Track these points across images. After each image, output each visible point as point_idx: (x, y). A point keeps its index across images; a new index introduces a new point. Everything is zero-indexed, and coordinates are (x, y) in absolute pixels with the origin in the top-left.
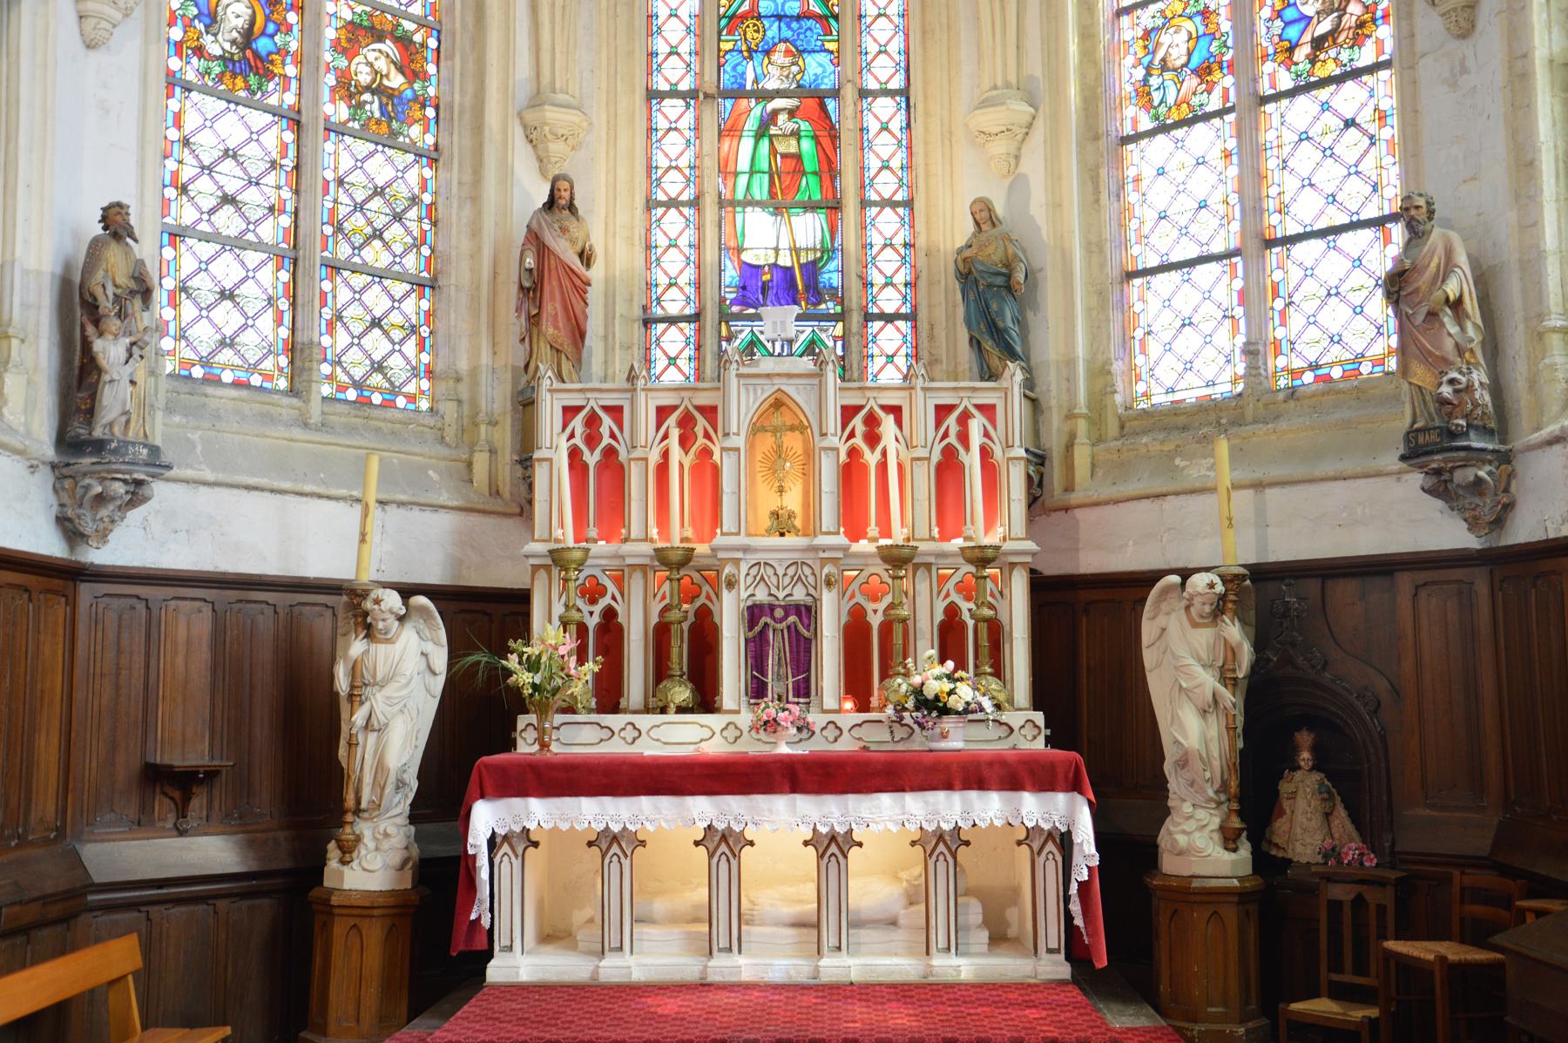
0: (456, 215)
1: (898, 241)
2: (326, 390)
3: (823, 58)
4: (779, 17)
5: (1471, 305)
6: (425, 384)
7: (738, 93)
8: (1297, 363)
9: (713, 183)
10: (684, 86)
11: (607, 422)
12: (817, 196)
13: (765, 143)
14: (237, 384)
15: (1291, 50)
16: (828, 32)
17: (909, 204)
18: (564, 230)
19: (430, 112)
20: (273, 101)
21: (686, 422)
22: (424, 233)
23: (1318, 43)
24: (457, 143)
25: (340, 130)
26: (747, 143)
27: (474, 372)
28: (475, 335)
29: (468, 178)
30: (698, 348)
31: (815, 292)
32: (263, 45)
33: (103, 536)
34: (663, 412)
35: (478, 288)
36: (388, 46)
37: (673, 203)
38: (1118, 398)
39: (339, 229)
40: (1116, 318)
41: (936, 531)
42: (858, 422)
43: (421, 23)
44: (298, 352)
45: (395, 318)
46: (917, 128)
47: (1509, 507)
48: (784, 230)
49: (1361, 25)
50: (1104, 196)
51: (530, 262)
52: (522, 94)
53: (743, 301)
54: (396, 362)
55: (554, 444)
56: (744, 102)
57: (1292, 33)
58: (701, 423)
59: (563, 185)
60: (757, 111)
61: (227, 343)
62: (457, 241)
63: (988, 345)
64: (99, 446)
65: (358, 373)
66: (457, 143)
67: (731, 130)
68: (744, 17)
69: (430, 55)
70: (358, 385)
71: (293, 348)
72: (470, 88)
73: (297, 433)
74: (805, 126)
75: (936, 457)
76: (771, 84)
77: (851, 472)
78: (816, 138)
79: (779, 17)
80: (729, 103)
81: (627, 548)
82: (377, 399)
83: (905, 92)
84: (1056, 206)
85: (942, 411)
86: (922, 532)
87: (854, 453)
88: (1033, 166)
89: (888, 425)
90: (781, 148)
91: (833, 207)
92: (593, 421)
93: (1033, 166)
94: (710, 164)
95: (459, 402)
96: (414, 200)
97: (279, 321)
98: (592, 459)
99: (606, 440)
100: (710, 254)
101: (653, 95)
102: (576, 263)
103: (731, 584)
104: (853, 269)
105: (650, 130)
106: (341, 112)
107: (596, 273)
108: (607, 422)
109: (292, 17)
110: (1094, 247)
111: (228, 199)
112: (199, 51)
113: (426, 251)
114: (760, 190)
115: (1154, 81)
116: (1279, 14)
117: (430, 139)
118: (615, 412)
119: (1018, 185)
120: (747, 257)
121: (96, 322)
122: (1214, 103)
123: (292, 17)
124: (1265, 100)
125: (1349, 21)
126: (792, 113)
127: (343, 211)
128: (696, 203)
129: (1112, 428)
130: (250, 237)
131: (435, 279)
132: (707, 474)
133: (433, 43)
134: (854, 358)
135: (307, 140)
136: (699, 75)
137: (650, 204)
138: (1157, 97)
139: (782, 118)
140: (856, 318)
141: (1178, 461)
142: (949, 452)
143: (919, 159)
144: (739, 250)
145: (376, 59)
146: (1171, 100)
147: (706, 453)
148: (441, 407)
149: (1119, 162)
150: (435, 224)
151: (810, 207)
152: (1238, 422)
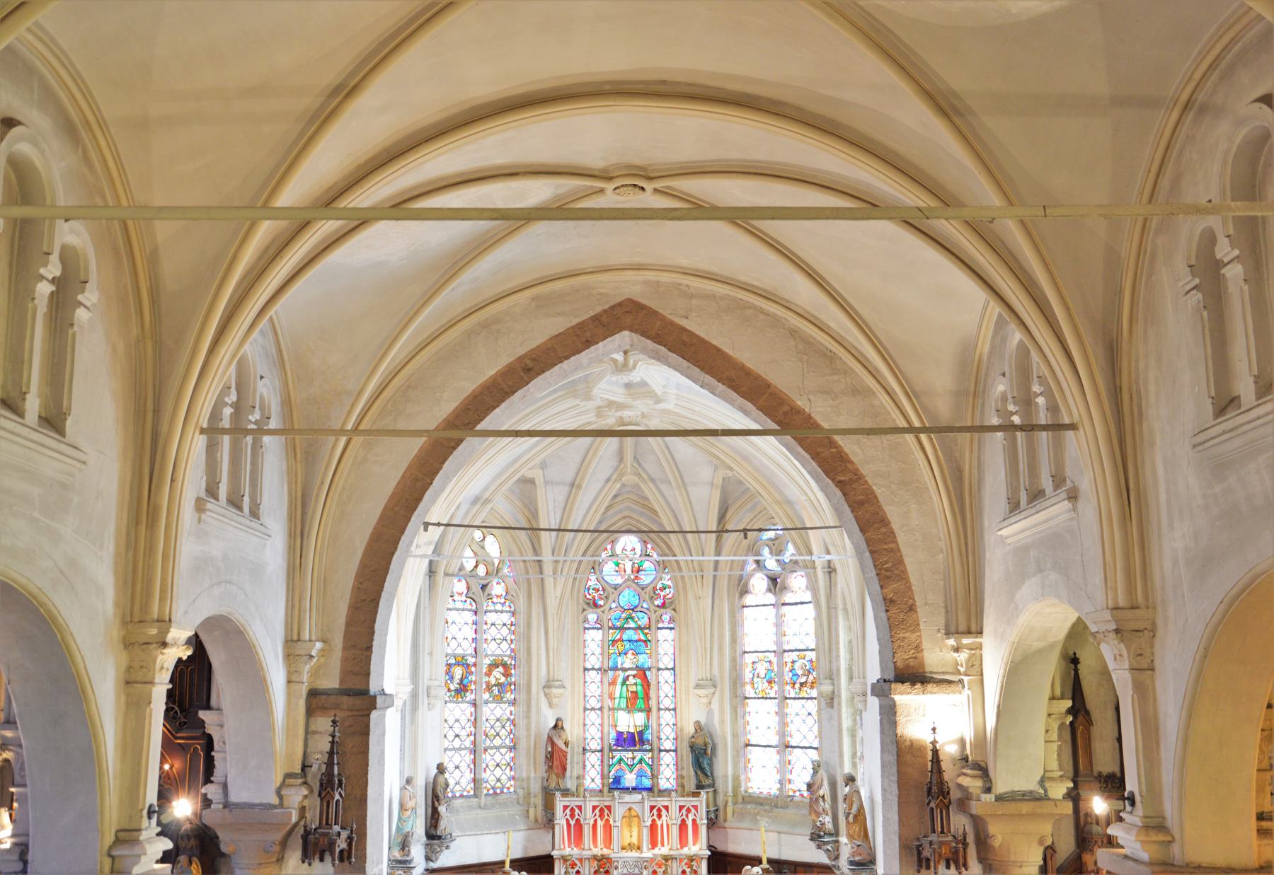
0: (521, 723)
1: (671, 723)
2: (485, 792)
3: (645, 656)
4: (630, 641)
5: (828, 798)
6: (512, 782)
7: (615, 669)
8: (795, 789)
9: (608, 703)
10: (596, 667)
11: (577, 811)
12: (643, 707)
13: (625, 687)
14: (461, 796)
15: (794, 684)
16: (647, 646)
17: (675, 709)
18: (560, 736)
19: (513, 687)
20: (468, 699)
21: (602, 810)
22: (511, 730)
23: (802, 684)
24: (522, 698)
25: (486, 702)
26: (618, 687)
27: (528, 778)
28: (528, 765)
29: (525, 709)
30: (602, 762)
31: (642, 742)
32: (465, 681)
33: (437, 859)
34: (594, 808)
35: (529, 749)
36: (501, 669)
37: (593, 709)
38: (742, 789)
39: (487, 736)
40: (742, 760)
41: (679, 847)
42: (655, 811)
43: (510, 657)
44: (476, 781)
45: (504, 762)
46: (677, 682)
47: (839, 855)
48: (632, 719)
49: (813, 683)
50: (739, 718)
51: (550, 749)
52: (543, 683)
53: (617, 745)
54: (504, 778)
55: (560, 820)
56: (617, 672)
57: (795, 678)
58: (606, 811)
59: (560, 722)
60: (621, 675)
61: (457, 783)
62: (522, 733)
63: (699, 772)
64: (439, 838)
65: (493, 784)
66: (522, 698)
67: (613, 683)
68: (617, 641)
69: (513, 667)
70: (493, 788)
71: (474, 780)
72: (526, 678)
73: (479, 811)
74: (639, 681)
75: (679, 822)
76: (627, 665)
77: (653, 827)
78: (642, 685)
79: (630, 641)
80: (612, 672)
81: (584, 853)
82: (498, 791)
83: (673, 669)
84: (722, 722)
85: (681, 808)
86: (674, 847)
87: (654, 821)
88: (715, 706)
89: (664, 811)
90: (630, 689)
91: (648, 710)
92: (572, 810)
93: (715, 706)
94: (606, 696)
95: (523, 789)
96: (508, 719)
97: (471, 772)
98: (572, 823)
99: (577, 817)
100: (606, 730)
101: (585, 669)
102: (563, 747)
103: (616, 868)
104: (655, 735)
105: (585, 682)
106: (486, 696)
107: (569, 750)
108: (577, 811)
109: (473, 669)
110: (735, 735)
111: (457, 736)
112: (449, 690)
113: (512, 736)
114: (623, 705)
115: (755, 680)
116: (791, 671)
117: (513, 696)
118: (580, 808)
119: (710, 712)
120: (619, 729)
121: (438, 801)
122: (772, 695)
123: (473, 669)
124: (786, 698)
125: (810, 680)
126: (634, 676)
127: (488, 729)
128: (601, 709)
129: (740, 800)
130: (463, 746)
131: (515, 745)
132: (608, 828)
133: (513, 662)
134: (655, 767)
135: (478, 710)
136: (602, 663)
137: (585, 709)
138: (756, 686)
139: (631, 678)
140: (656, 753)
141: (758, 817)
142: (683, 821)
143: (678, 695)
144: (616, 726)
145: (497, 673)
146: (760, 689)
147: (608, 821)
148: (518, 791)
149: (744, 705)
150: (514, 726)
151: (640, 710)
152: (776, 806)
